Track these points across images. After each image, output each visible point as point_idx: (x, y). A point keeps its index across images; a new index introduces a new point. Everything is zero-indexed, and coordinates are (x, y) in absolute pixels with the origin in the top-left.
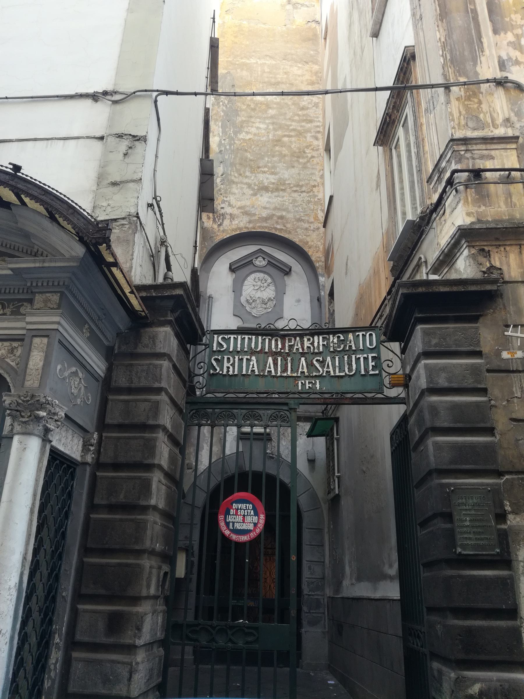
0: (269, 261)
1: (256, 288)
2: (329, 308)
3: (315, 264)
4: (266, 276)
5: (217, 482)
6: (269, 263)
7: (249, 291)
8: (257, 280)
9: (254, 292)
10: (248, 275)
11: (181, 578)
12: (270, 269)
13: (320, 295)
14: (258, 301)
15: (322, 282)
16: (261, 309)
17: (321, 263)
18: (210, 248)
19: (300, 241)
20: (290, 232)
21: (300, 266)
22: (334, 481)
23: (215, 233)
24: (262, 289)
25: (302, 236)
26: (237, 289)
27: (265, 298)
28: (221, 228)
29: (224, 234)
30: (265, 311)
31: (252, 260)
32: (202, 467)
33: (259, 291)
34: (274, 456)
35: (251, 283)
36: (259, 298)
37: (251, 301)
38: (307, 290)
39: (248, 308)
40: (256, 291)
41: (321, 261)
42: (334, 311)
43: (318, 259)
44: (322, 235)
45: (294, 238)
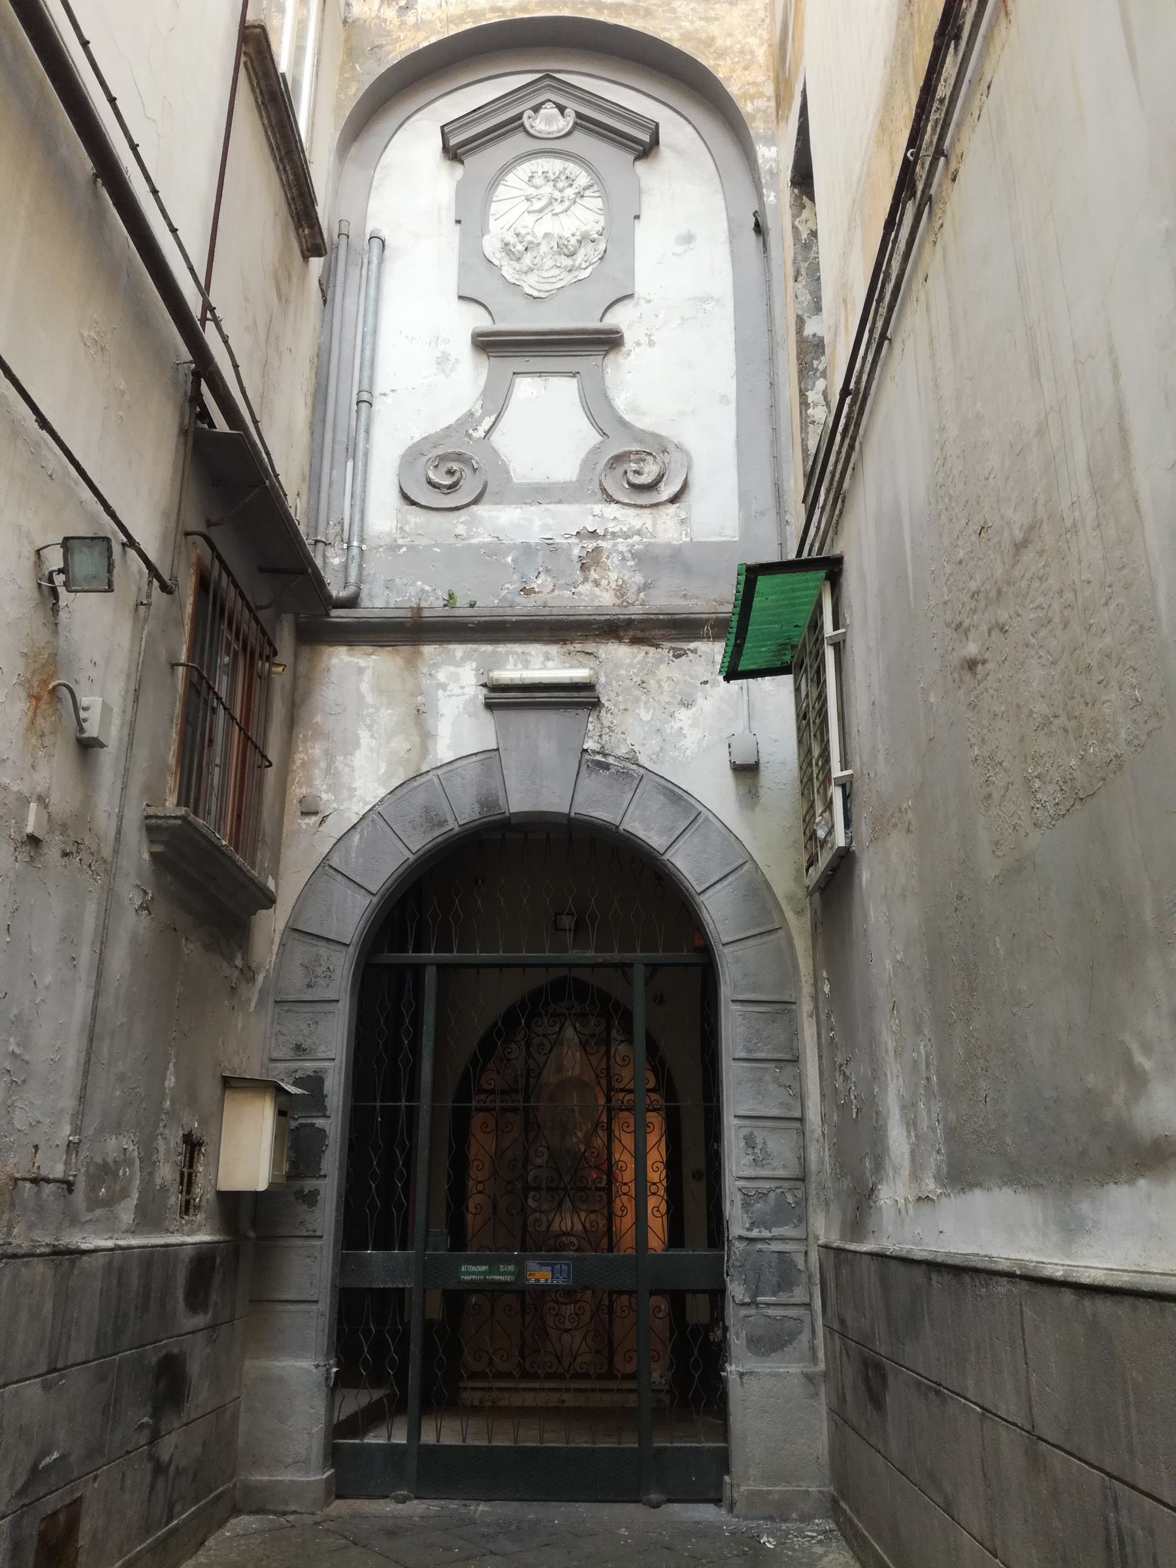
0: (579, 115)
1: (537, 205)
2: (794, 228)
3: (740, 105)
4: (572, 168)
5: (409, 855)
6: (583, 123)
7: (509, 218)
8: (538, 181)
9: (529, 220)
10: (506, 169)
11: (256, 1193)
12: (583, 143)
13: (762, 204)
14: (544, 248)
15: (767, 160)
16: (556, 272)
17: (761, 103)
18: (369, 80)
19: (686, 36)
20: (648, 13)
21: (689, 128)
22: (829, 806)
23: (389, 33)
24: (558, 208)
25: (692, 22)
26: (470, 216)
27: (567, 234)
28: (411, 18)
29: (421, 35)
30: (569, 278)
31: (519, 117)
32: (355, 808)
33: (548, 217)
34: (611, 760)
35: (518, 193)
36: (546, 235)
37: (520, 247)
38: (719, 201)
39: (508, 273)
40: (536, 216)
41: (761, 95)
42: (814, 234)
43: (752, 91)
44: (762, 14)
45: (663, 30)
